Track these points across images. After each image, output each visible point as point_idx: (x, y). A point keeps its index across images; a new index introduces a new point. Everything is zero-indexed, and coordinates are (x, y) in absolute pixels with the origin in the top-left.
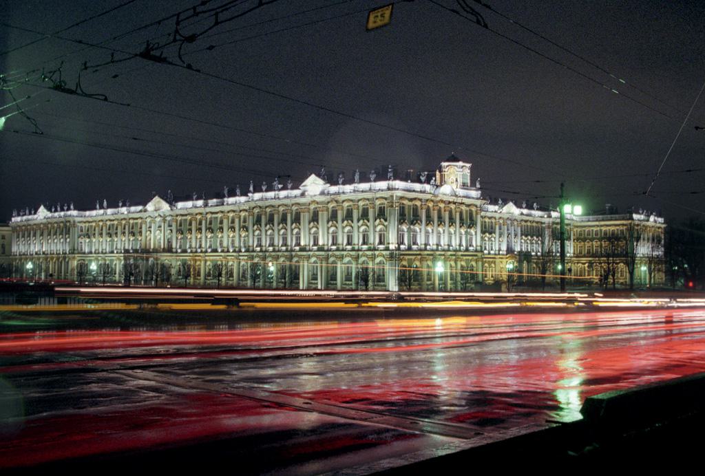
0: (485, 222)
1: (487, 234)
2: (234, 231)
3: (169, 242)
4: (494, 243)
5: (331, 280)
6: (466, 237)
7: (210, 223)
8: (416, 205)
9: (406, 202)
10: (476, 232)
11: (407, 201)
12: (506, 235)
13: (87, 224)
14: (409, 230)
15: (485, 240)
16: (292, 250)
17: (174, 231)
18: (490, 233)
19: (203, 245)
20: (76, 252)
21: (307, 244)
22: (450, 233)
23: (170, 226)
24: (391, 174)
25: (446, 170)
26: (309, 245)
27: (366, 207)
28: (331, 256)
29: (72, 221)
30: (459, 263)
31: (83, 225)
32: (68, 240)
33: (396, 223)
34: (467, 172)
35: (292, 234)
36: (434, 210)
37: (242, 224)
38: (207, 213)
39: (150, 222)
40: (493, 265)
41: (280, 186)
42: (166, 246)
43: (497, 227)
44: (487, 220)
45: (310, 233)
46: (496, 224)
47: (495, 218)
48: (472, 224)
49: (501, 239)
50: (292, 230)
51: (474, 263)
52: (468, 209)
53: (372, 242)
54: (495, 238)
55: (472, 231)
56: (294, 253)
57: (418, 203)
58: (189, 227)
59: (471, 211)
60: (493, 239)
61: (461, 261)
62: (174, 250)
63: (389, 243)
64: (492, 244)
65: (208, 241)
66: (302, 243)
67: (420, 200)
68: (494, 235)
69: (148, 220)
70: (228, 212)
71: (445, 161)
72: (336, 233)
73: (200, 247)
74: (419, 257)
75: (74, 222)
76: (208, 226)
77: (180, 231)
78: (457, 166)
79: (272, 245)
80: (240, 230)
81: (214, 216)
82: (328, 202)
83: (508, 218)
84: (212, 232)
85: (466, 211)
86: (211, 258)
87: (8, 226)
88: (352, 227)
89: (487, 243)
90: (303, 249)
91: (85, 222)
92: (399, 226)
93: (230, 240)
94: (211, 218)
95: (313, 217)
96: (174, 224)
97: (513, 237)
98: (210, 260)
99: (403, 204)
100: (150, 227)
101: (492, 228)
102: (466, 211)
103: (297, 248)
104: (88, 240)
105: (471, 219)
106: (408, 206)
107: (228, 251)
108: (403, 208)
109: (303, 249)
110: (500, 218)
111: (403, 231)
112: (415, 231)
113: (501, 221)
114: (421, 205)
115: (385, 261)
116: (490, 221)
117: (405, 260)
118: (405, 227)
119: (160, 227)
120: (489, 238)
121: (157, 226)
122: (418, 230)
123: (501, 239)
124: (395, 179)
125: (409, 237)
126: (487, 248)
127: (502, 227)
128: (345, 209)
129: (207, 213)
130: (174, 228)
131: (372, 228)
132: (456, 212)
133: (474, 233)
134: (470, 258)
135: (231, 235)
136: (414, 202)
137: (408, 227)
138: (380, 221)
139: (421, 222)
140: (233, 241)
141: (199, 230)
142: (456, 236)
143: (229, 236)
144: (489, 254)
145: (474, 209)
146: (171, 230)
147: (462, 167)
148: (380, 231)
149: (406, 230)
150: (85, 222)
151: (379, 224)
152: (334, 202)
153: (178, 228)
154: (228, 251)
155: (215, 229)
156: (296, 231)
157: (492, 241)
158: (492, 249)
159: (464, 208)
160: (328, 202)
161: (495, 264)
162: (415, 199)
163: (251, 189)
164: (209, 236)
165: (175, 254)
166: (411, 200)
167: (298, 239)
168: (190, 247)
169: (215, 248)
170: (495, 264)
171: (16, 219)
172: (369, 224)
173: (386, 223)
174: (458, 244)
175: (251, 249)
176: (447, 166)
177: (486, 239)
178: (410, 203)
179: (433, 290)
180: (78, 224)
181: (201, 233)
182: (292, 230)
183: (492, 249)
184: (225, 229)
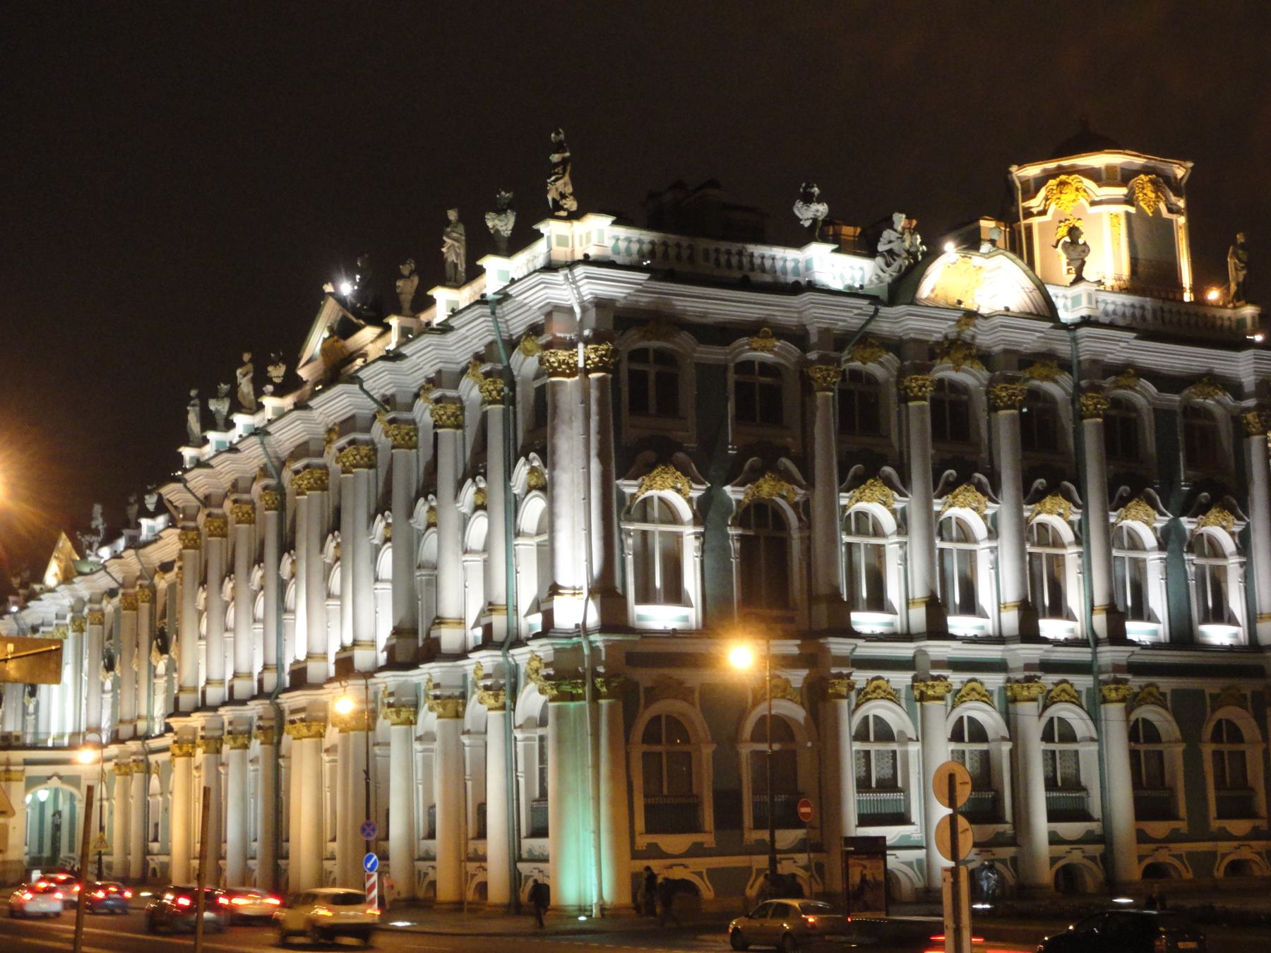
108: (668, 385)
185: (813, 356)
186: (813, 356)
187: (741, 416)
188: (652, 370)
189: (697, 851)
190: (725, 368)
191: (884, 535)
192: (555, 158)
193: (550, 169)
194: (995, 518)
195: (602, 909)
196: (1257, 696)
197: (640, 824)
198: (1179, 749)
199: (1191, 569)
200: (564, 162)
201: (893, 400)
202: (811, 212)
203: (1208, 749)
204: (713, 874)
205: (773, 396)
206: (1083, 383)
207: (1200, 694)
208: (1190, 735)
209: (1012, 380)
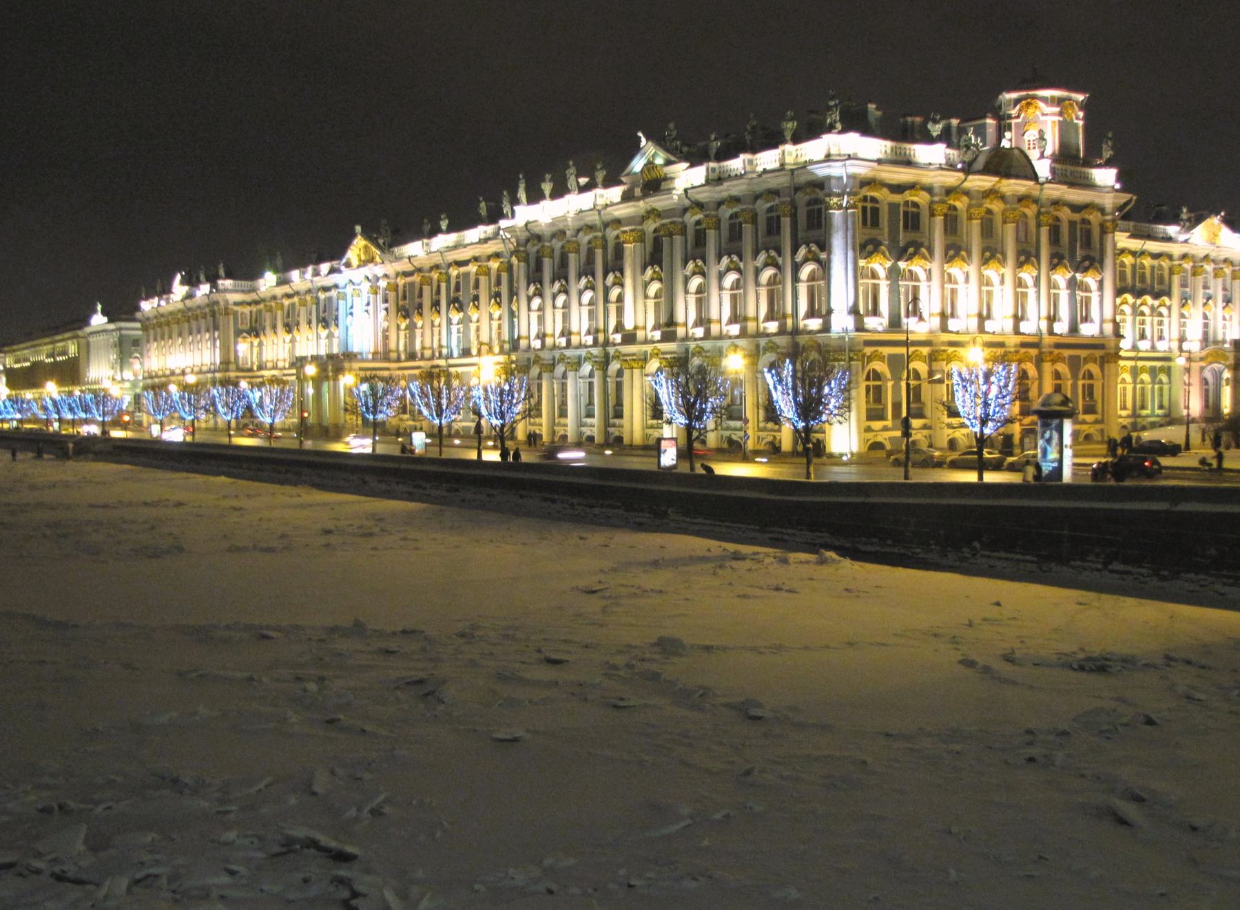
0: (1143, 267)
1: (1148, 299)
2: (499, 304)
3: (386, 338)
4: (1166, 320)
6: (1072, 297)
7: (457, 289)
8: (915, 205)
9: (882, 195)
10: (1101, 283)
11: (885, 191)
12: (1201, 301)
13: (254, 309)
14: (894, 274)
15: (1142, 314)
16: (607, 343)
17: (393, 310)
18: (1156, 296)
19: (444, 343)
20: (232, 367)
21: (641, 324)
22: (1019, 283)
23: (386, 301)
24: (836, 116)
25: (1014, 112)
26: (645, 328)
27: (774, 214)
28: (693, 355)
29: (222, 303)
30: (1047, 367)
31: (247, 310)
32: (218, 343)
33: (850, 254)
34: (1078, 118)
35: (606, 300)
36: (970, 218)
38: (450, 265)
40: (1164, 378)
41: (583, 181)
42: (380, 349)
43: (1176, 279)
44: (1147, 262)
45: (646, 297)
46: (1171, 272)
47: (1170, 257)
48: (1092, 261)
49: (1184, 311)
50: (607, 291)
51: (1094, 368)
52: (1077, 217)
53: (789, 310)
54: (1169, 308)
55: (1090, 280)
57: (922, 198)
58: (417, 300)
59: (1084, 221)
60: (1164, 310)
61: (1054, 362)
62: (393, 355)
63: (830, 311)
64: (1160, 323)
65: (454, 328)
66: (629, 325)
67: (929, 189)
68: (1165, 299)
70: (489, 258)
71: (1009, 91)
74: (925, 351)
75: (227, 302)
77: (405, 312)
78: (1044, 100)
79: (566, 333)
81: (462, 270)
82: (685, 210)
83: (1207, 257)
84: (460, 309)
85: (1072, 224)
86: (460, 370)
87: (134, 320)
89: (1148, 319)
90: (629, 338)
91: (249, 304)
92: (862, 263)
93: (495, 324)
94: (458, 277)
95: (652, 255)
96: (392, 295)
97: (1220, 304)
98: (458, 376)
99: (873, 200)
101: (1161, 281)
102: (1072, 224)
104: (256, 342)
105: (1087, 243)
106: (893, 207)
108: (875, 212)
109: (629, 338)
110: (1184, 257)
111: (874, 275)
112: (912, 276)
113: (1188, 266)
114: (932, 202)
116: (1155, 262)
117: (882, 359)
118: (880, 265)
119: (368, 304)
120: (1153, 309)
122: (922, 275)
123: (1184, 311)
124: (844, 131)
125: (894, 291)
126: (1148, 333)
127: (1190, 279)
129: (450, 265)
132: (1039, 225)
133: (1093, 285)
134: (1083, 353)
135: (496, 314)
136: (910, 196)
137: (888, 264)
138: (810, 251)
139: (931, 250)
140: (500, 327)
141: (436, 304)
142: (1039, 292)
143: (491, 318)
144: (1153, 348)
145: (1094, 218)
146: (386, 309)
147: (1059, 102)
148: (812, 278)
149: (882, 273)
150: (249, 304)
151: (806, 260)
152: (697, 210)
153: (401, 303)
156: (614, 293)
157: (1160, 315)
158: (1161, 338)
159: (1065, 214)
160: (685, 210)
161: (1169, 375)
162: (912, 186)
164: (455, 321)
166: (898, 188)
167: (620, 312)
170: (1169, 375)
171: (147, 306)
172: (780, 261)
173: (823, 256)
174: (1044, 313)
176: (1017, 101)
177: (1146, 309)
178: (896, 198)
179: (746, 458)
180: (236, 308)
181: (439, 312)
183: (1161, 338)
184: (483, 298)
185: (936, 199)
186: (936, 199)
187: (906, 227)
188: (869, 205)
189: (885, 429)
190: (899, 205)
191: (956, 283)
192: (832, 103)
193: (829, 108)
194: (1003, 276)
195: (852, 454)
196: (1102, 358)
197: (864, 417)
198: (1070, 383)
199: (1078, 298)
200: (836, 105)
201: (965, 216)
202: (936, 129)
203: (1080, 383)
204: (891, 439)
205: (916, 217)
206: (1043, 210)
207: (1078, 357)
208: (1075, 376)
209: (1015, 210)
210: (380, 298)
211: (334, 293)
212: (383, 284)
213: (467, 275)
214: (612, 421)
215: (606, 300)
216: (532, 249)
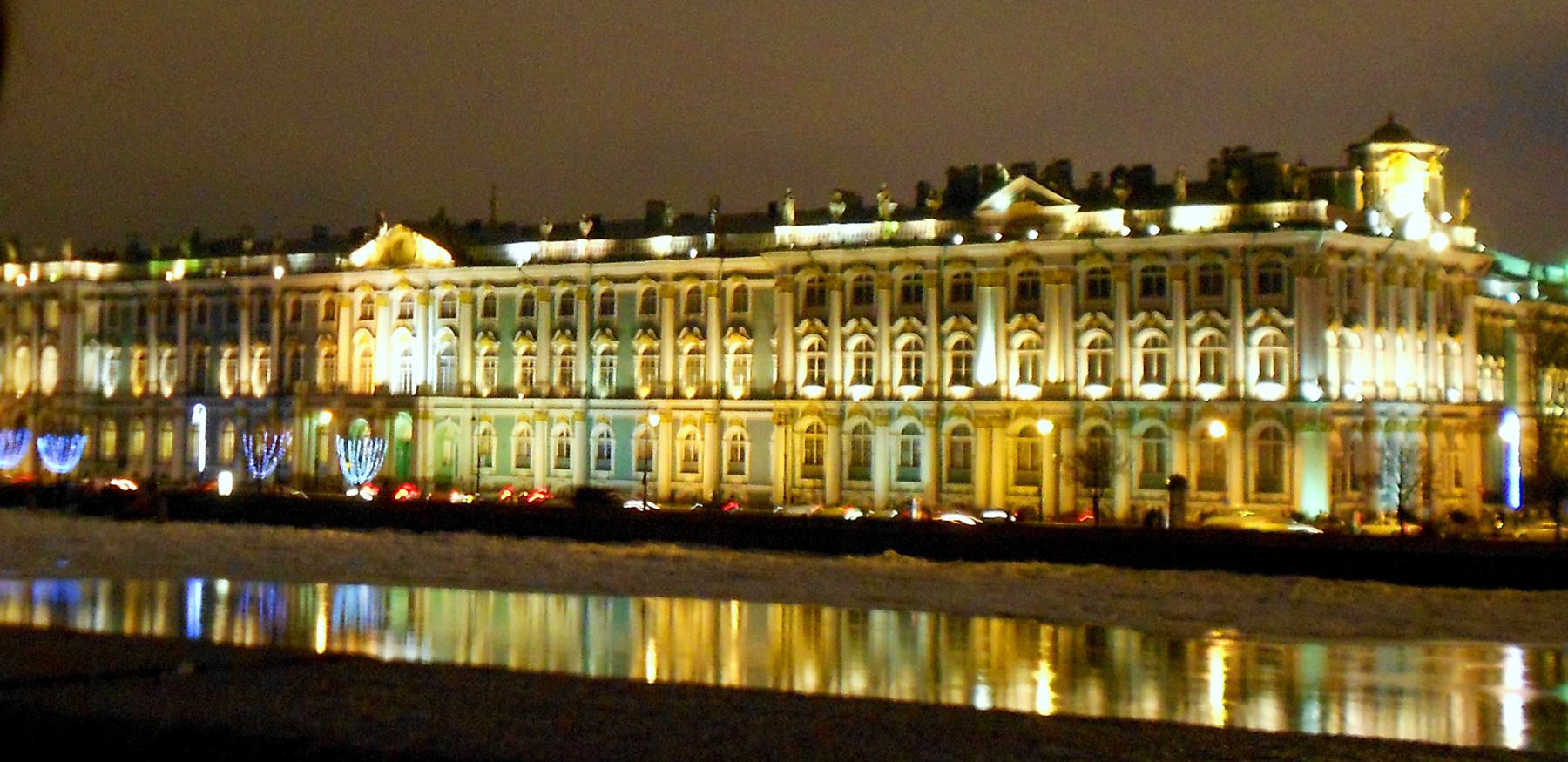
5: (852, 477)
35: (941, 347)
37: (729, 314)
38: (594, 280)
39: (368, 301)
56: (948, 406)
62: (467, 389)
69: (359, 295)
72: (968, 346)
73: (566, 377)
76: (729, 314)
80: (723, 333)
81: (618, 288)
88: (1110, 332)
100: (367, 316)
103: (961, 391)
107: (678, 395)
115: (822, 423)
121: (396, 313)
128: (849, 287)
129: (594, 280)
130: (463, 320)
131: (934, 338)
152: (1099, 256)
154: (678, 395)
155: (626, 327)
163: (790, 211)
165: (470, 401)
168: (527, 378)
169: (627, 384)
175: (789, 390)
182: (942, 338)
210: (434, 310)
211: (323, 298)
212: (440, 292)
213: (630, 296)
214: (945, 486)
215: (941, 347)
216: (803, 278)
